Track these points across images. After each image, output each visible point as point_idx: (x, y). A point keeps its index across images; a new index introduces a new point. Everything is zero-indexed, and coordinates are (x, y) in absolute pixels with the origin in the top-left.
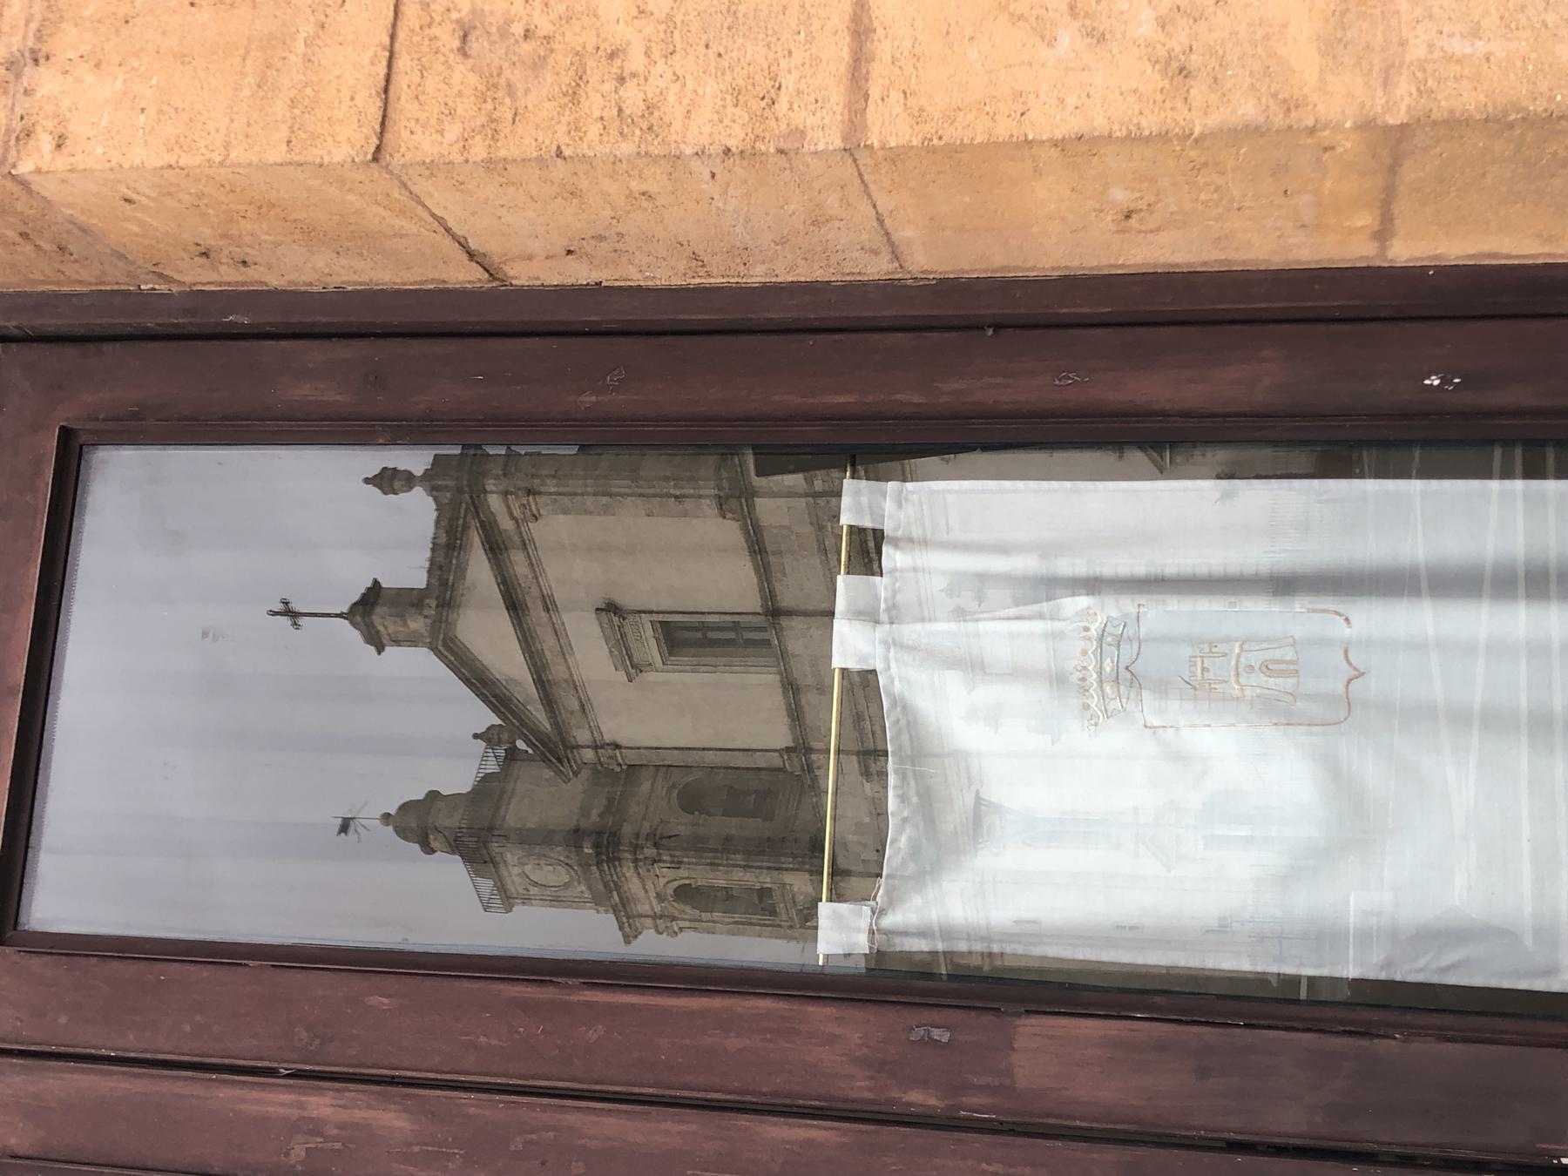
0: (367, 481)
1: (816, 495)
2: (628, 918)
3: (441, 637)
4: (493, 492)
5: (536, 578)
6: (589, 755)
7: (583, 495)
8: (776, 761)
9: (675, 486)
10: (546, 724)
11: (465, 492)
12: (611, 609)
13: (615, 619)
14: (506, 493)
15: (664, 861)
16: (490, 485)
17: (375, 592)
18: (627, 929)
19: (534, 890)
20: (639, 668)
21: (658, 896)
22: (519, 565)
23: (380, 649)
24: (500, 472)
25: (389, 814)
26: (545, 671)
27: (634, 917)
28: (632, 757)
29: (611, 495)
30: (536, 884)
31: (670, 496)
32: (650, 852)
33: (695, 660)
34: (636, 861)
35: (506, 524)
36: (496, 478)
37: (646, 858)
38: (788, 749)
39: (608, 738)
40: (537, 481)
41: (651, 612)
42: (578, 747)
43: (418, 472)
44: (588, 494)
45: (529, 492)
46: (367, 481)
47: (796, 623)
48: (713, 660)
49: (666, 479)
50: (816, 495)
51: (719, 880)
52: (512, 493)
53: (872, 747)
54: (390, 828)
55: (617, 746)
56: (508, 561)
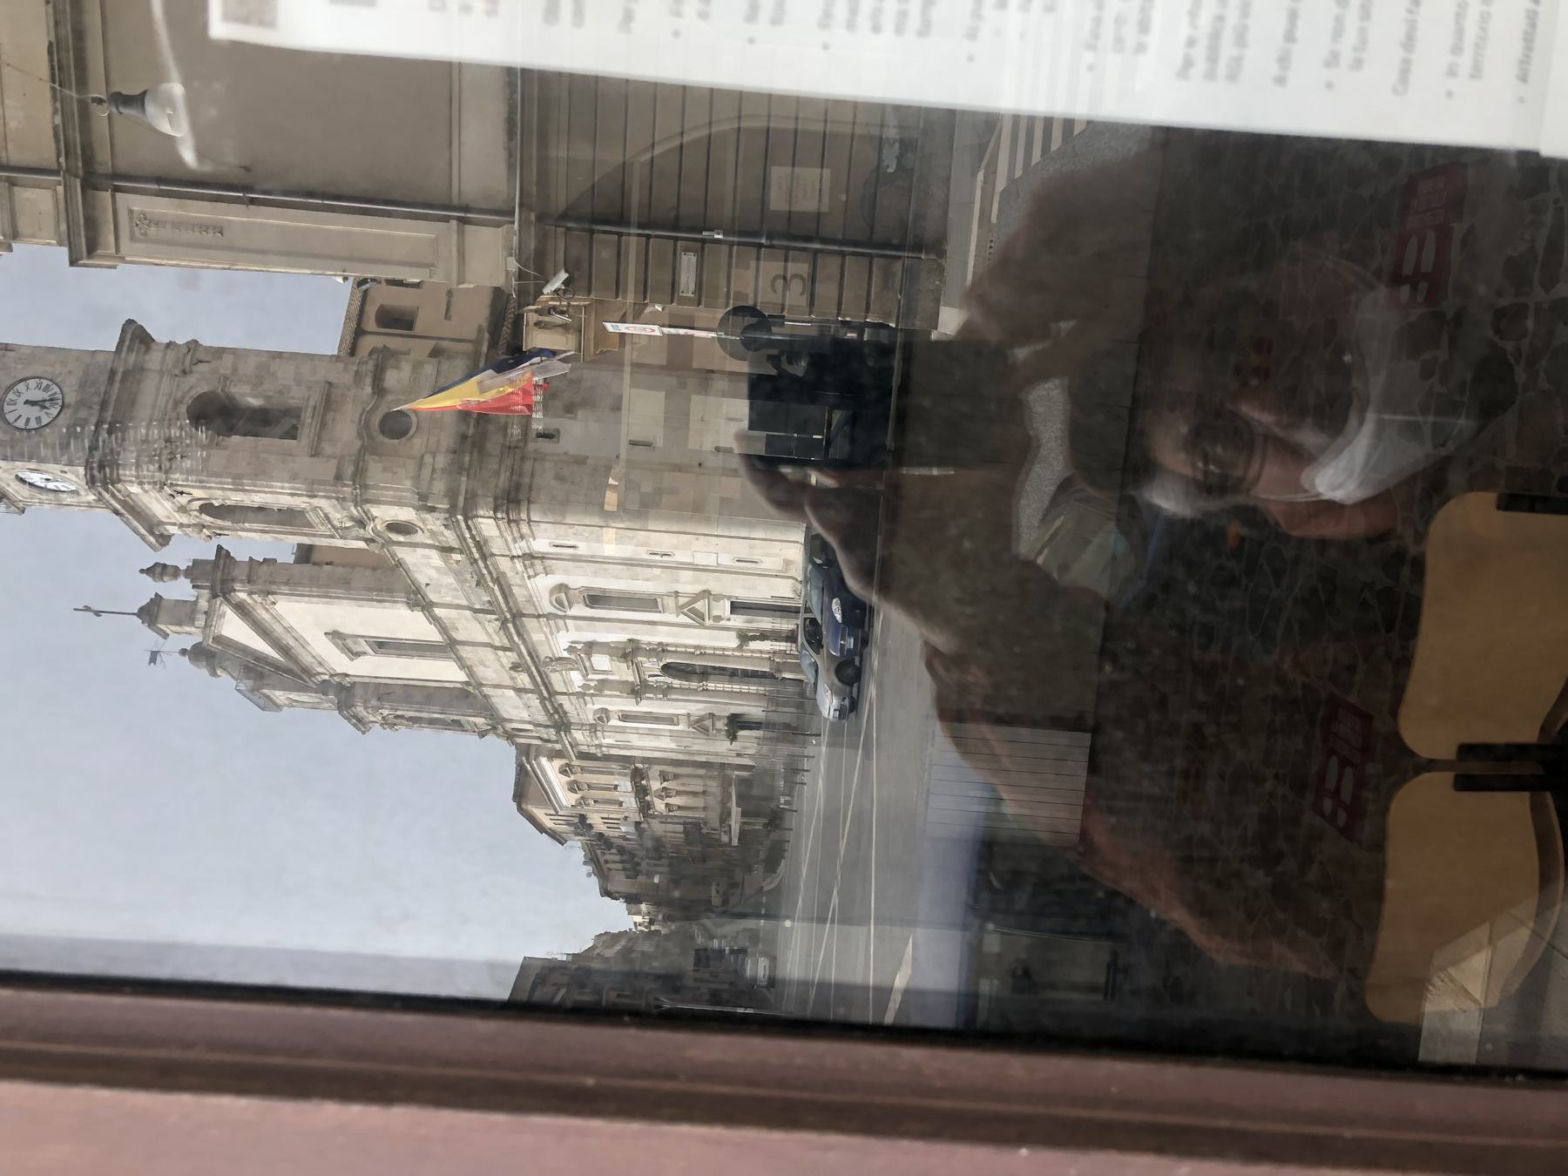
0: (142, 571)
1: (476, 611)
2: (363, 725)
3: (211, 640)
4: (240, 591)
5: (279, 621)
6: (327, 677)
7: (309, 596)
8: (459, 686)
9: (377, 595)
10: (291, 665)
11: (219, 596)
12: (336, 636)
13: (340, 642)
14: (250, 594)
15: (386, 708)
16: (237, 586)
17: (158, 599)
18: (363, 729)
19: (294, 704)
20: (358, 654)
21: (384, 718)
22: (262, 614)
23: (165, 636)
24: (244, 578)
25: (185, 649)
26: (290, 650)
27: (368, 723)
28: (357, 680)
29: (330, 597)
30: (297, 701)
31: (373, 600)
32: (374, 702)
33: (398, 652)
34: (366, 708)
35: (249, 601)
36: (242, 581)
37: (372, 707)
38: (467, 683)
39: (339, 672)
40: (274, 588)
41: (363, 637)
42: (319, 674)
43: (183, 567)
44: (314, 596)
45: (269, 593)
46: (142, 571)
47: (467, 648)
48: (410, 653)
49: (370, 590)
50: (476, 611)
51: (424, 715)
52: (255, 593)
53: (522, 687)
54: (187, 657)
55: (347, 675)
56: (256, 614)
